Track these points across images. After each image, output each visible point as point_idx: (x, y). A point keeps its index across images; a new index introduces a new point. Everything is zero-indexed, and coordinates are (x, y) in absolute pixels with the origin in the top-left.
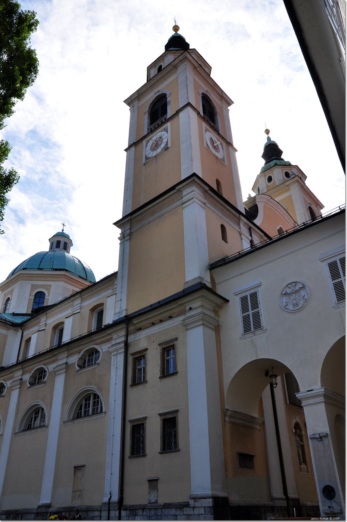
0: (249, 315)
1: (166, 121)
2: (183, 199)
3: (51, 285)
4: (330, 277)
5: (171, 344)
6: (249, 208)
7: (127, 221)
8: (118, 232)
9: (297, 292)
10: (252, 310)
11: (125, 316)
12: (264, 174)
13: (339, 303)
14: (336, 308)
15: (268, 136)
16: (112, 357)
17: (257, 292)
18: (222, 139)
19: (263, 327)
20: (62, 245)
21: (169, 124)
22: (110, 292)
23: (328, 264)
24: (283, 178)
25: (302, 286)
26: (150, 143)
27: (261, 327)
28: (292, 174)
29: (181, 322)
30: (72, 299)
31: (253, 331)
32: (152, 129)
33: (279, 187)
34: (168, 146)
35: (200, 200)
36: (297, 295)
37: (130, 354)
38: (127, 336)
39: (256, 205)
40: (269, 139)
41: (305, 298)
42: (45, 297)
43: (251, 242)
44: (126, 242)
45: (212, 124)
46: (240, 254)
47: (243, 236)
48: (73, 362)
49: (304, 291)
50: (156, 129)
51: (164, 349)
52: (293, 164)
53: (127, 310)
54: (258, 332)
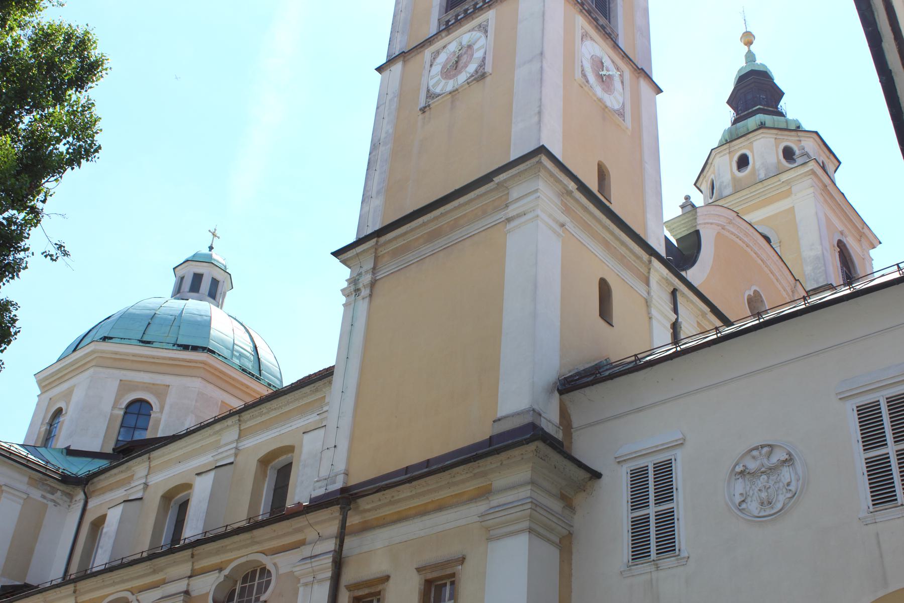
0: (647, 519)
1: (485, 6)
2: (511, 208)
3: (169, 386)
4: (861, 440)
5: (449, 571)
6: (678, 239)
7: (368, 249)
8: (342, 273)
9: (772, 470)
10: (656, 504)
11: (342, 489)
12: (730, 148)
13: (876, 511)
14: (869, 522)
15: (749, 51)
16: (301, 589)
17: (673, 460)
18: (623, 59)
19: (679, 550)
20: (205, 285)
22: (312, 418)
23: (857, 407)
24: (776, 161)
25: (787, 457)
26: (442, 58)
27: (675, 550)
28: (803, 155)
29: (476, 519)
30: (217, 427)
31: (655, 559)
32: (450, 23)
33: (765, 183)
34: (484, 69)
35: (550, 216)
36: (775, 477)
37: (345, 586)
38: (341, 538)
39: (697, 233)
40: (750, 57)
41: (789, 488)
42: (150, 415)
43: (675, 326)
44: (361, 301)
45: (602, 21)
46: (640, 360)
47: (654, 312)
48: (204, 592)
49: (791, 469)
50: (458, 22)
51: (428, 583)
52: (806, 126)
53: (347, 475)
54: (668, 562)
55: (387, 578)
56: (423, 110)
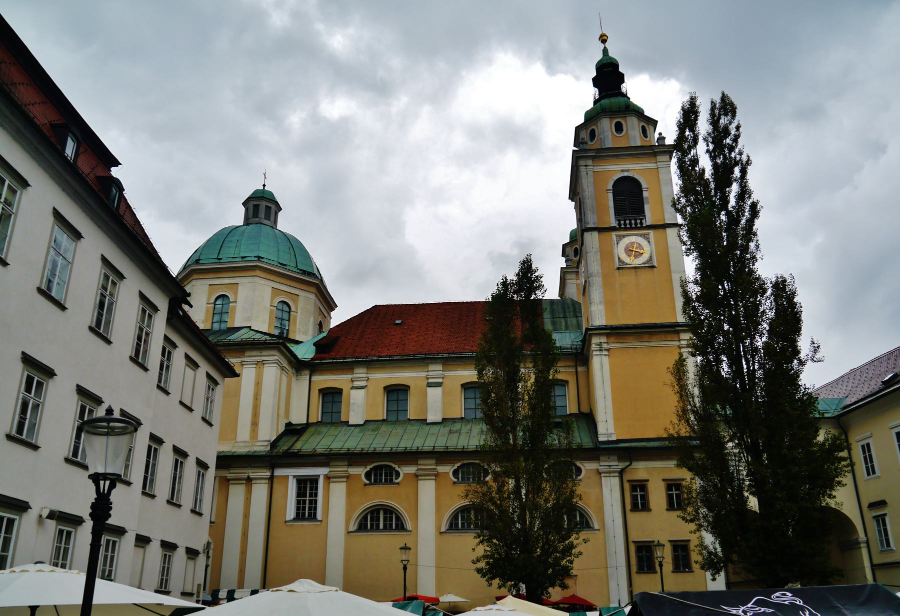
16: (602, 478)
21: (651, 233)
50: (631, 228)
55: (648, 480)
56: (619, 268)
